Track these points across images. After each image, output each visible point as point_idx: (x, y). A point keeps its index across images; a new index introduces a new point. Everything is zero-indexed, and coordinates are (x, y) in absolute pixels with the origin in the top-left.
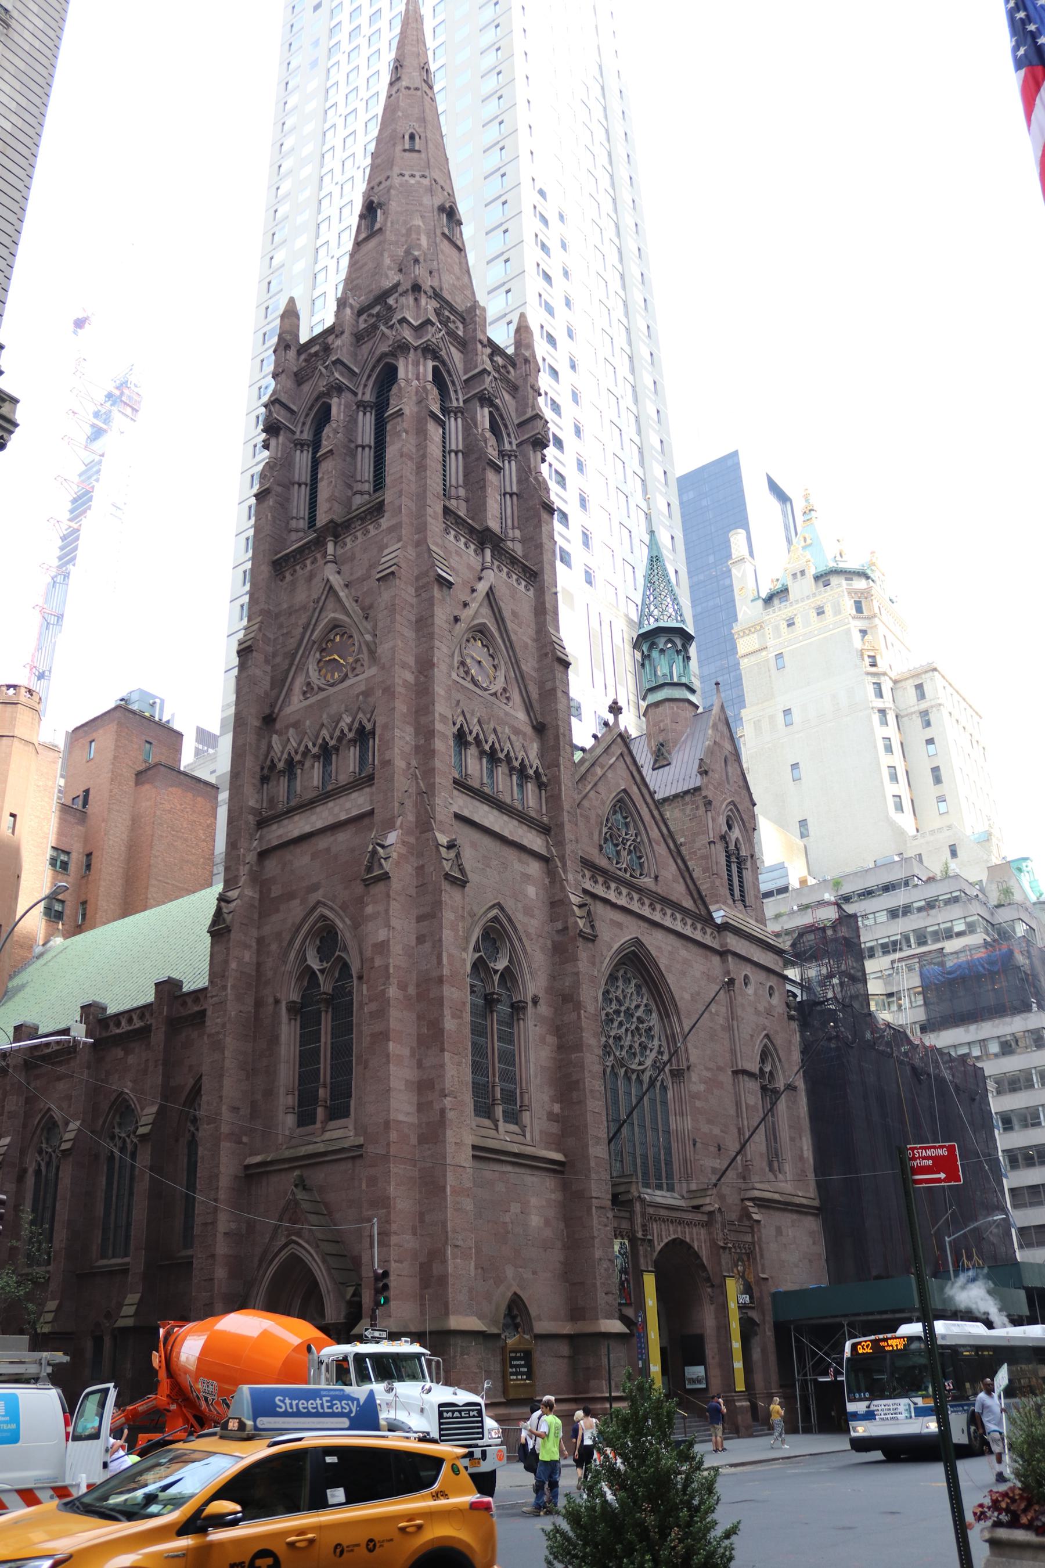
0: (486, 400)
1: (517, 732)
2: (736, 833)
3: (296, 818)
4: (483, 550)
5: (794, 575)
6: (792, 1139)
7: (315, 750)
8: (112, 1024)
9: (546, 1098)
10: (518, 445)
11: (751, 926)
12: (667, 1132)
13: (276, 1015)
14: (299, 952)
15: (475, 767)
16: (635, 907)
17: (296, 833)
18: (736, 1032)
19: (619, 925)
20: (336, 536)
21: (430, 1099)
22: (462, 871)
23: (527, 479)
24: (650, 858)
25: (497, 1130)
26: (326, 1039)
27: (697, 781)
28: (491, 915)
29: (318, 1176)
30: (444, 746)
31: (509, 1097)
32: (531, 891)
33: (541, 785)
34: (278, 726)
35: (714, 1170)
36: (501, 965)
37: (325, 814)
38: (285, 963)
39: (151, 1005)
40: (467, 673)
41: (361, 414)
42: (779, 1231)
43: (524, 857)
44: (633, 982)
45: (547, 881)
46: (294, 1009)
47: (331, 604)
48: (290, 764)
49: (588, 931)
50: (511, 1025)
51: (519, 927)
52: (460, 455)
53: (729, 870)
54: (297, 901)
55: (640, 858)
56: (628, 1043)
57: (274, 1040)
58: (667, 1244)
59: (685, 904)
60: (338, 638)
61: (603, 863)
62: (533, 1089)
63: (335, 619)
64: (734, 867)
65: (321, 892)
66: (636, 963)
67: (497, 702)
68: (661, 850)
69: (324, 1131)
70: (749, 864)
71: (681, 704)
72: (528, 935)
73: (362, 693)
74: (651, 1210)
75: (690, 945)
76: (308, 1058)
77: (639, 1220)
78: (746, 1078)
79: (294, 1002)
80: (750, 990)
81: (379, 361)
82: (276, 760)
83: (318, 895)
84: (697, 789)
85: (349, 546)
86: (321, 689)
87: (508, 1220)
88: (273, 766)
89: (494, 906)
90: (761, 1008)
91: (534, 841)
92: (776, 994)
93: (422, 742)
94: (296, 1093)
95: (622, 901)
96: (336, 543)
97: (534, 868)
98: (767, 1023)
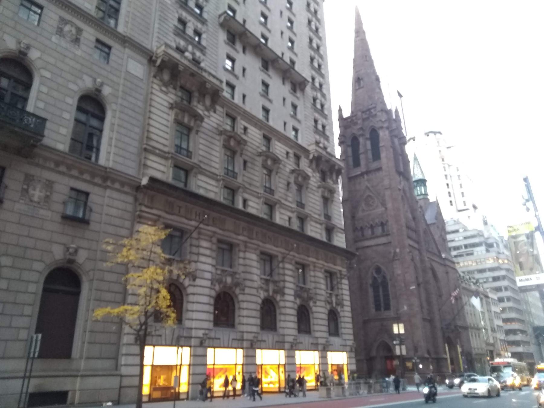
26: (381, 293)
27: (435, 221)
30: (404, 228)
68: (432, 241)
91: (416, 245)
97: (416, 252)
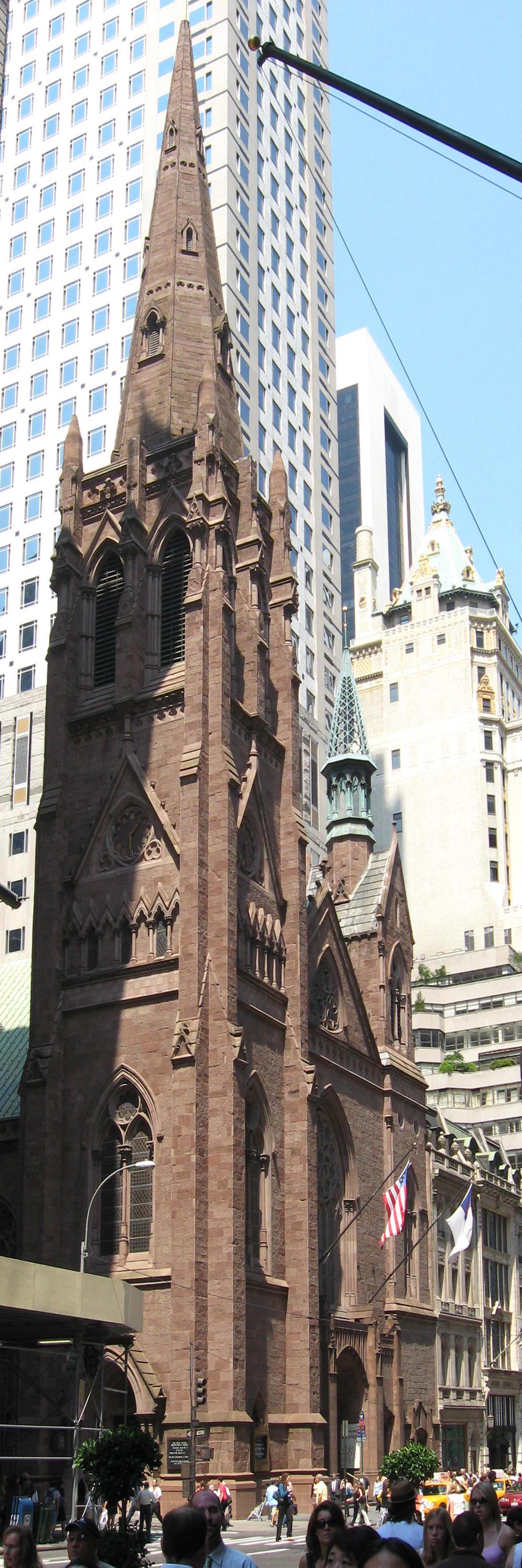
3: (99, 986)
17: (98, 1001)
20: (133, 714)
41: (150, 578)
48: (92, 930)
60: (132, 817)
63: (132, 798)
88: (75, 932)
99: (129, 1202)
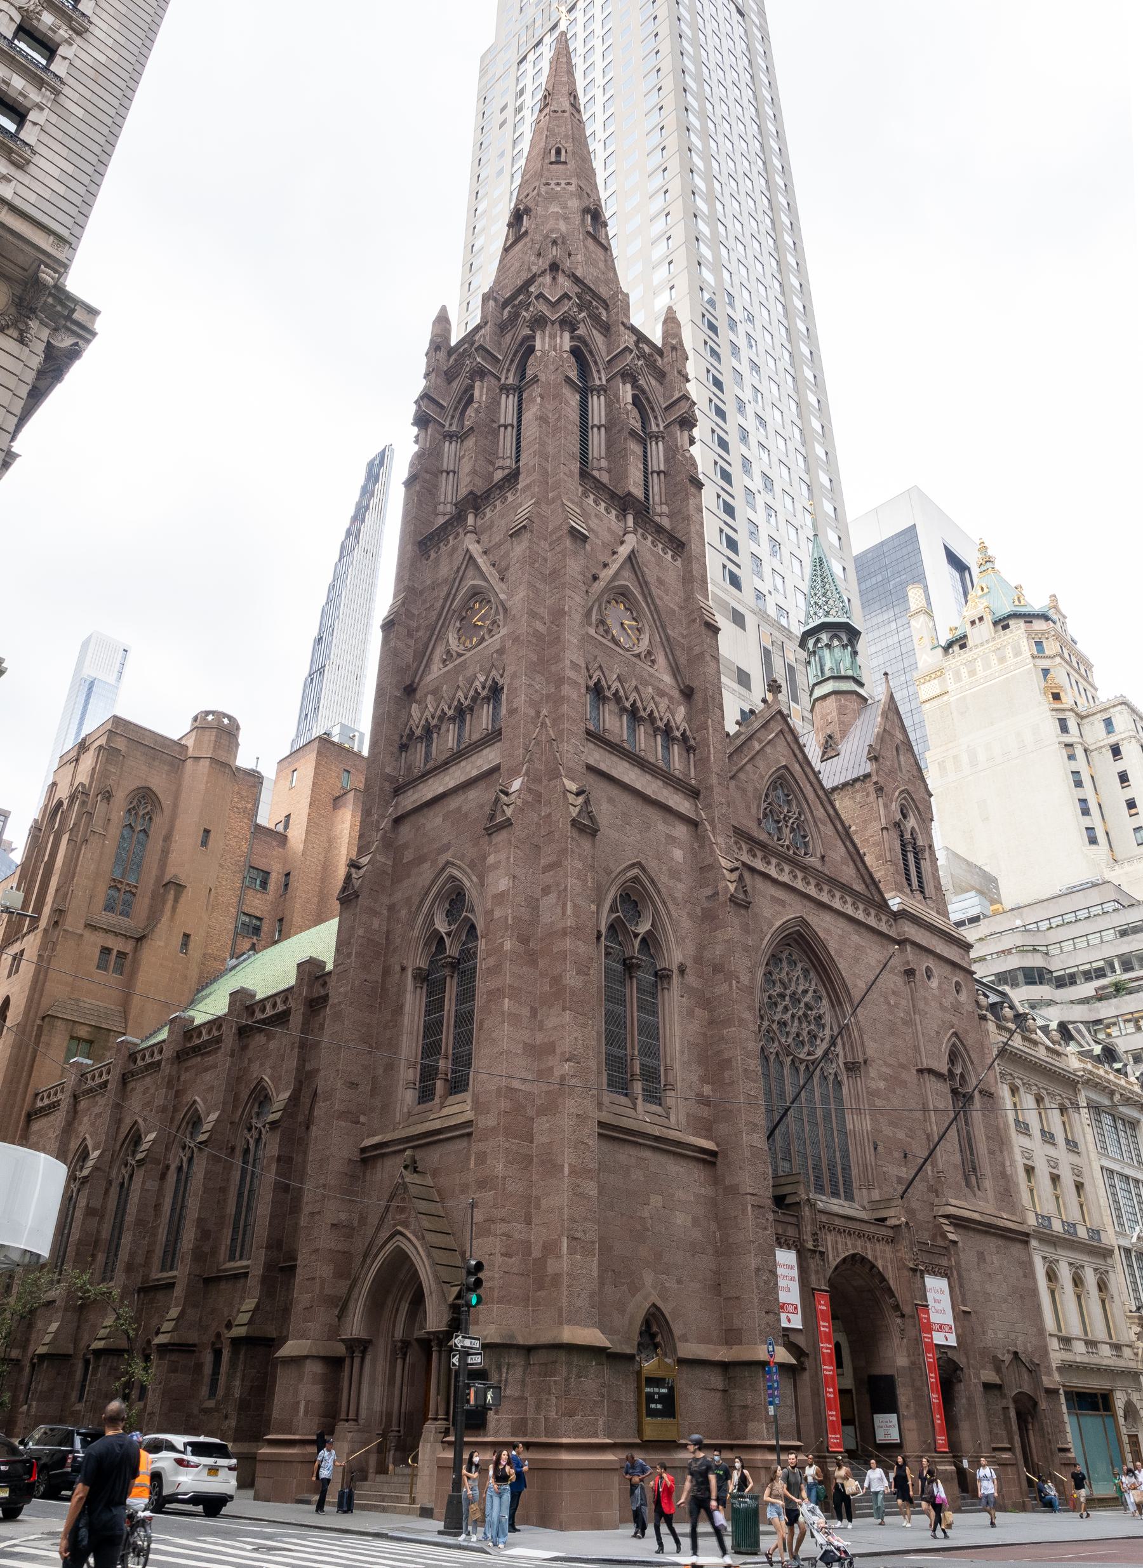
0: (629, 376)
1: (662, 694)
2: (912, 822)
3: (431, 781)
4: (625, 516)
5: (973, 623)
6: (991, 1152)
7: (450, 713)
8: (257, 1010)
9: (695, 1079)
10: (665, 427)
11: (930, 915)
12: (843, 1132)
13: (401, 986)
14: (427, 915)
15: (614, 724)
16: (799, 884)
17: (430, 796)
18: (919, 1027)
19: (782, 903)
21: (550, 1064)
22: (592, 818)
23: (674, 457)
24: (815, 837)
25: (635, 1109)
26: (450, 1006)
27: (868, 767)
28: (630, 874)
29: (432, 1157)
31: (651, 1075)
32: (678, 854)
33: (689, 749)
34: (418, 695)
35: (900, 1180)
36: (644, 928)
37: (458, 773)
38: (413, 928)
39: (292, 988)
40: (607, 631)
41: (504, 396)
42: (981, 1256)
43: (670, 819)
44: (800, 965)
45: (696, 846)
46: (421, 977)
47: (470, 573)
49: (742, 896)
50: (654, 995)
51: (663, 890)
52: (603, 430)
53: (905, 860)
54: (427, 865)
55: (804, 837)
56: (794, 1030)
57: (399, 1010)
58: (844, 1260)
59: (856, 887)
61: (763, 837)
62: (677, 1066)
63: (474, 586)
64: (911, 856)
65: (450, 853)
66: (799, 943)
67: (639, 662)
69: (442, 1107)
70: (927, 855)
71: (849, 696)
72: (674, 899)
73: (497, 651)
74: (824, 1218)
75: (862, 930)
76: (432, 1029)
77: (808, 1229)
78: (933, 1079)
79: (419, 968)
80: (934, 983)
81: (521, 345)
82: (414, 728)
83: (448, 856)
84: (867, 776)
85: (488, 516)
86: (459, 655)
87: (646, 1214)
89: (633, 865)
90: (947, 1004)
91: (683, 805)
92: (964, 991)
93: (553, 690)
94: (419, 1067)
95: (785, 878)
96: (476, 516)
97: (681, 831)
98: (955, 1021)
99: (452, 1028)
